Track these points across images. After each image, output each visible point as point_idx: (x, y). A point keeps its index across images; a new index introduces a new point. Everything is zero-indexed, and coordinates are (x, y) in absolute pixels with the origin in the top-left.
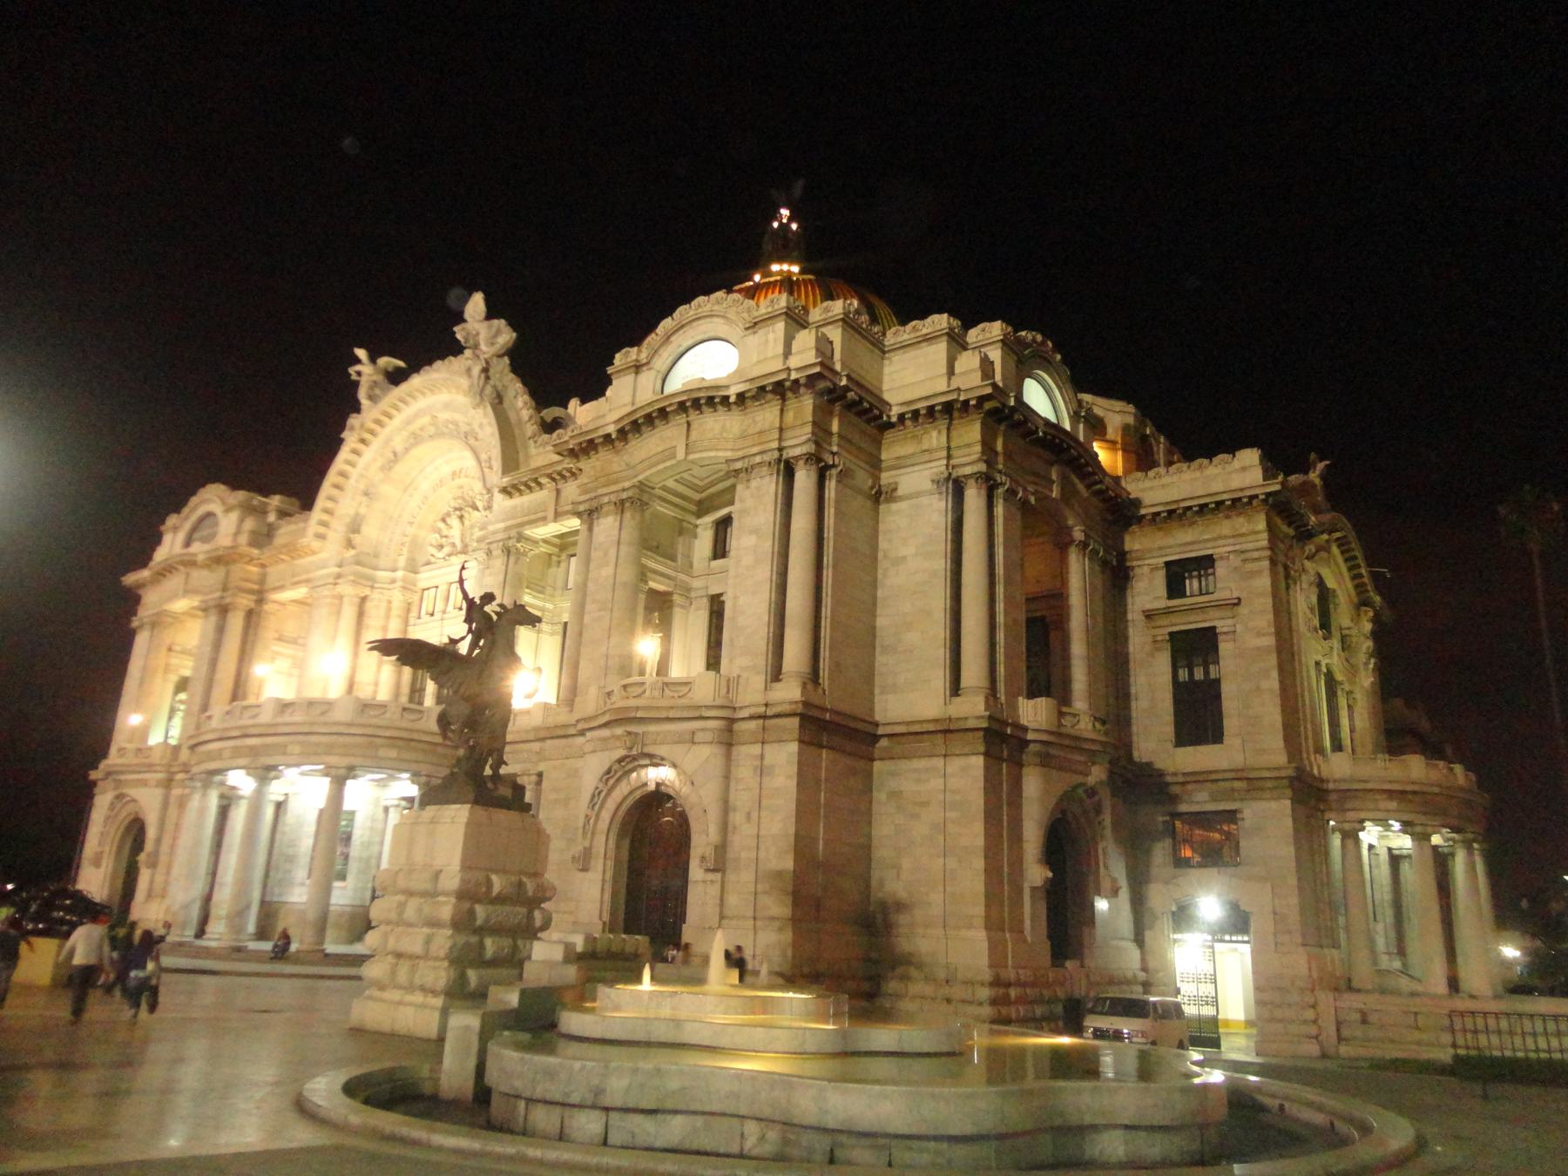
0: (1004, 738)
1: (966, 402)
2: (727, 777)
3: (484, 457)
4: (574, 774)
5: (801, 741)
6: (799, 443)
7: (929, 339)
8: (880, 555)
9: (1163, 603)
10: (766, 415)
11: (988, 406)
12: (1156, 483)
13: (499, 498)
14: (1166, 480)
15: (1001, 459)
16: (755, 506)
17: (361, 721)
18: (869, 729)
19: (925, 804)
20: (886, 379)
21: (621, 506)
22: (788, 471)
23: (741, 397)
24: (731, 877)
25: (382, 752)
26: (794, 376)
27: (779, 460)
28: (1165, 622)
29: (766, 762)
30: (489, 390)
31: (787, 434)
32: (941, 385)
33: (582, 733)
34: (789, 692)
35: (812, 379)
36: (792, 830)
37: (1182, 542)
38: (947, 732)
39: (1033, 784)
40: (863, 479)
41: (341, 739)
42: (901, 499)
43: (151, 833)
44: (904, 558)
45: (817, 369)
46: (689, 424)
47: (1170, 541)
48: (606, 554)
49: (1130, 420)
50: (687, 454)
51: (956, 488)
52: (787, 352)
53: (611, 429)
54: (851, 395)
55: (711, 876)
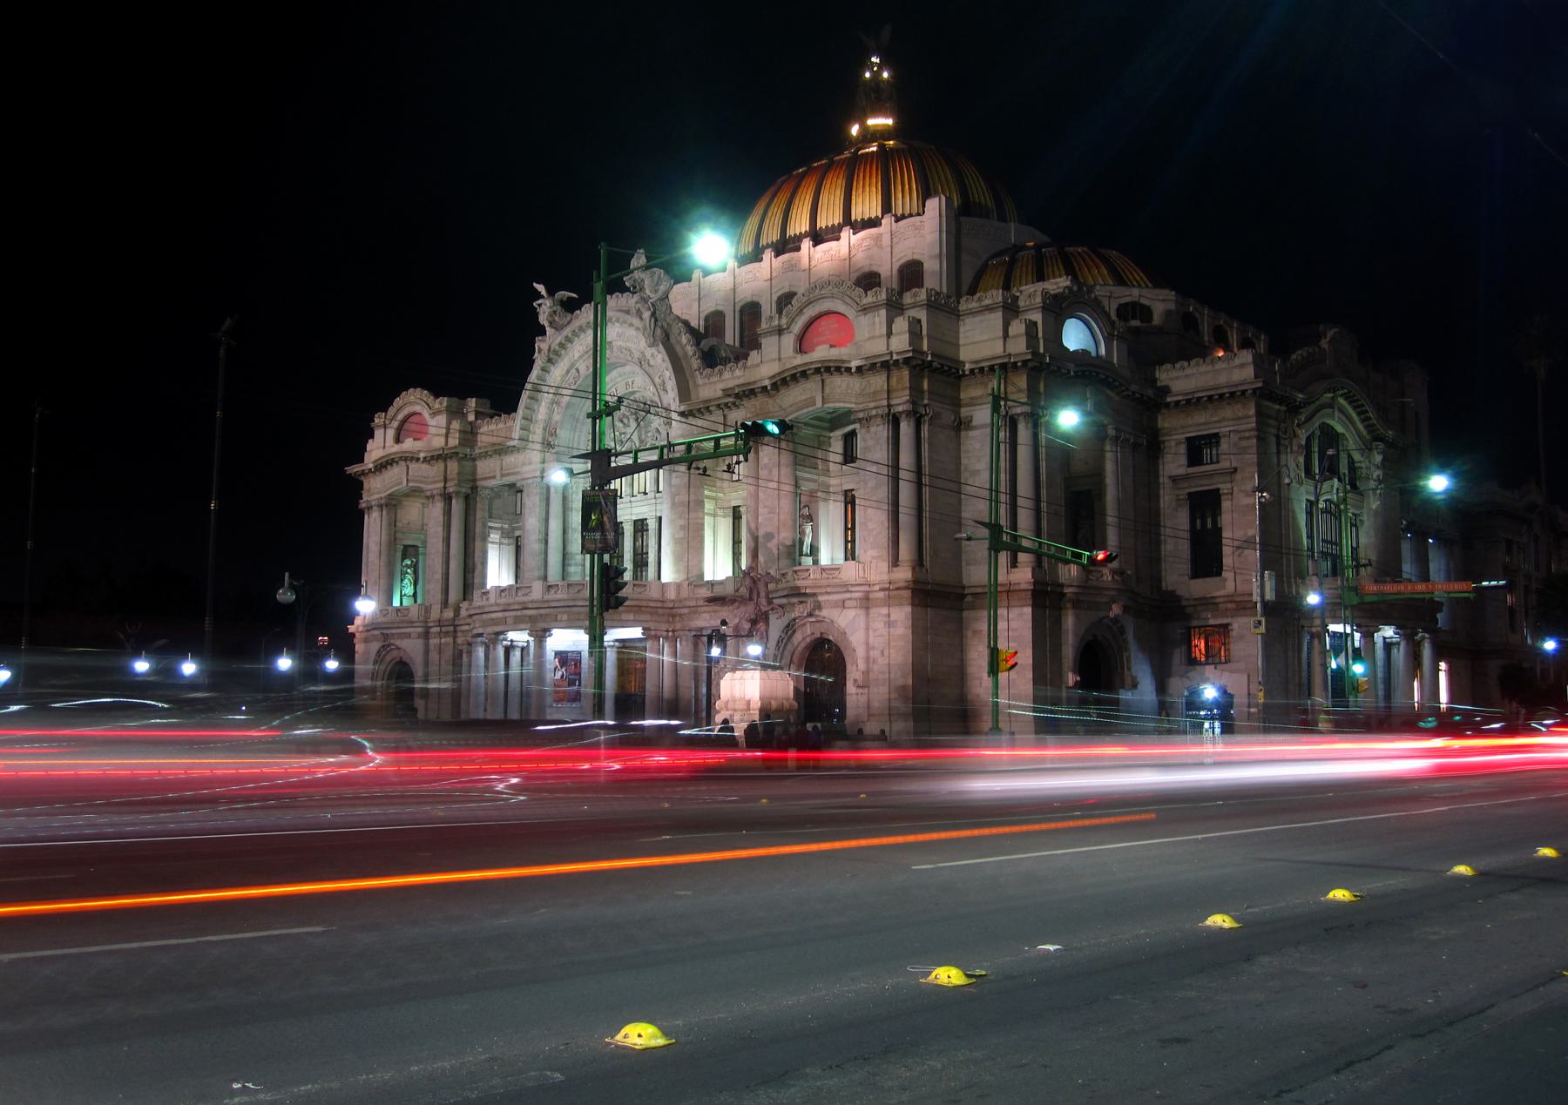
1: (1015, 364)
3: (657, 380)
6: (901, 402)
7: (989, 309)
9: (1182, 471)
10: (878, 381)
12: (1181, 373)
14: (1188, 371)
16: (874, 443)
23: (859, 369)
30: (659, 331)
31: (893, 395)
32: (998, 349)
34: (904, 574)
35: (907, 361)
37: (1198, 423)
39: (1069, 621)
40: (947, 417)
42: (975, 428)
49: (1172, 306)
52: (889, 334)
53: (767, 383)
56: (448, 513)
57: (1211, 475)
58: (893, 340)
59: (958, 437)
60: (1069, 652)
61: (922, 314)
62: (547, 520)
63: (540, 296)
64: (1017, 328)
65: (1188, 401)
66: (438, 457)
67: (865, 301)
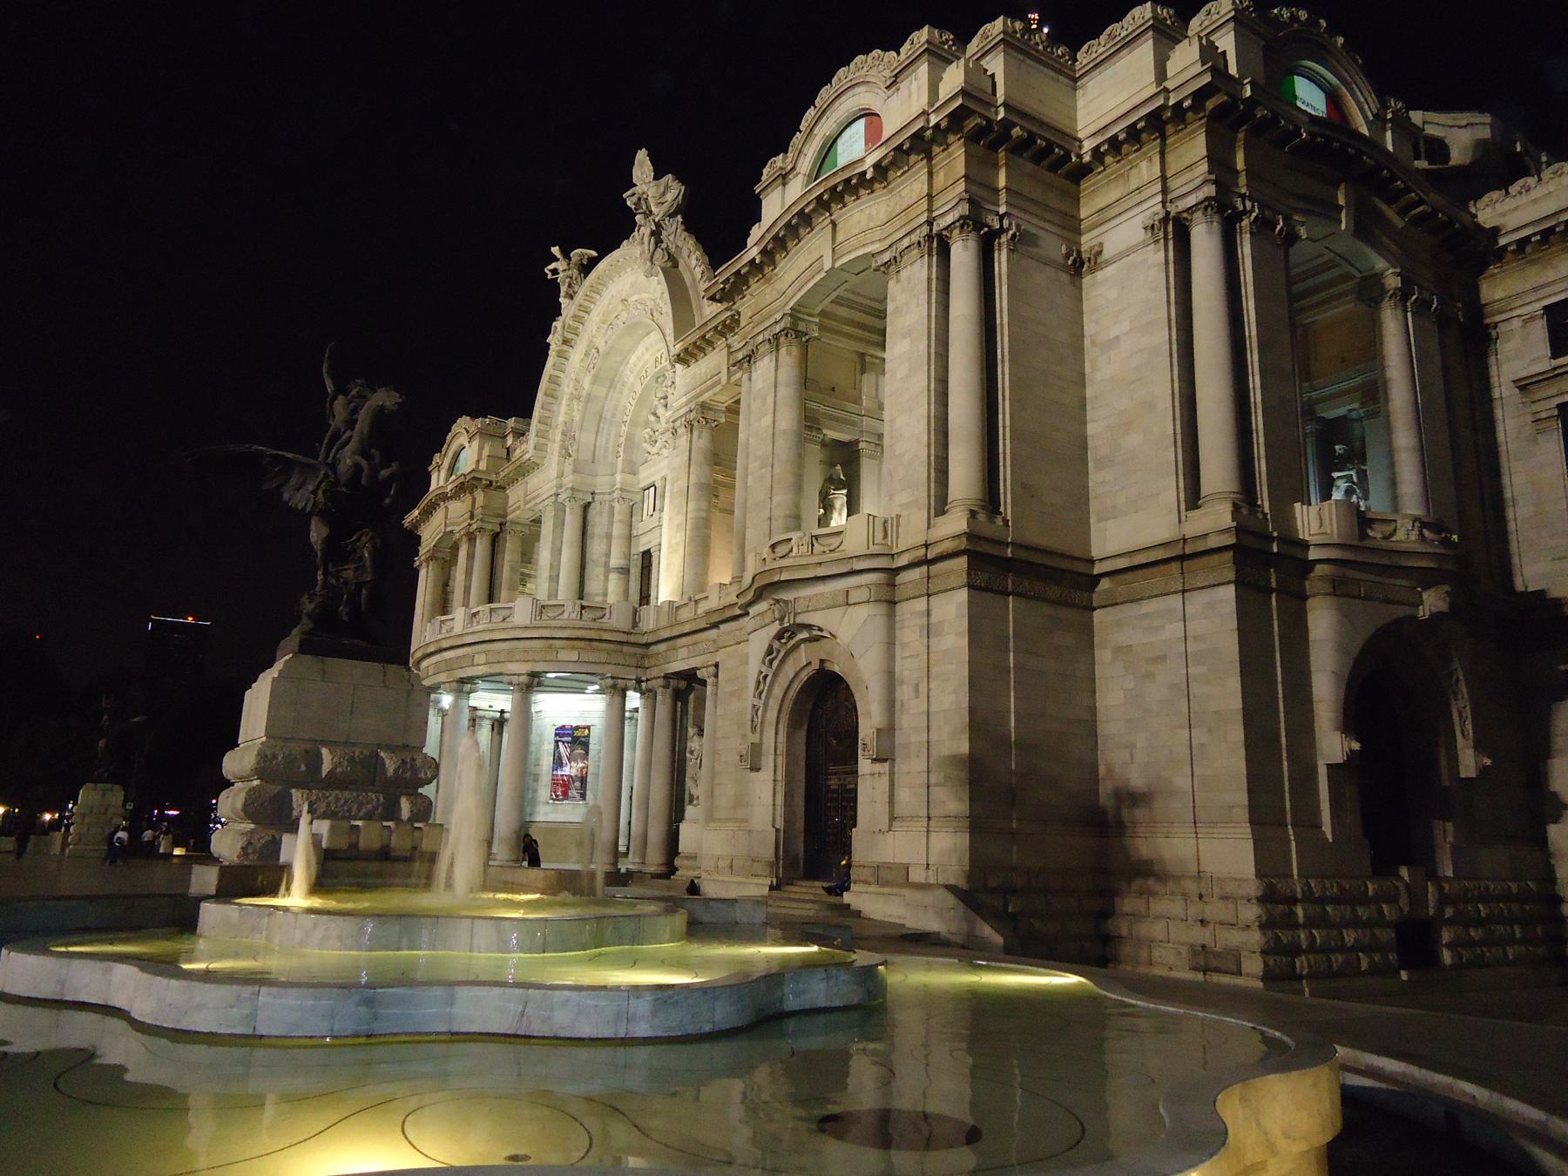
0: (1269, 560)
1: (1179, 104)
2: (891, 643)
5: (971, 586)
7: (1129, 43)
8: (1087, 342)
9: (1545, 365)
10: (912, 186)
11: (1210, 104)
12: (1524, 199)
15: (1243, 180)
17: (540, 623)
19: (1162, 658)
20: (1080, 114)
22: (940, 247)
24: (901, 766)
25: (563, 655)
26: (933, 120)
27: (930, 237)
28: (1553, 391)
29: (933, 620)
31: (936, 204)
34: (955, 523)
38: (1180, 558)
39: (1323, 623)
40: (1054, 247)
41: (522, 644)
42: (1109, 262)
44: (1117, 338)
46: (834, 224)
47: (1551, 275)
48: (764, 400)
50: (834, 261)
51: (1176, 231)
54: (1016, 132)
55: (878, 767)
56: (471, 557)
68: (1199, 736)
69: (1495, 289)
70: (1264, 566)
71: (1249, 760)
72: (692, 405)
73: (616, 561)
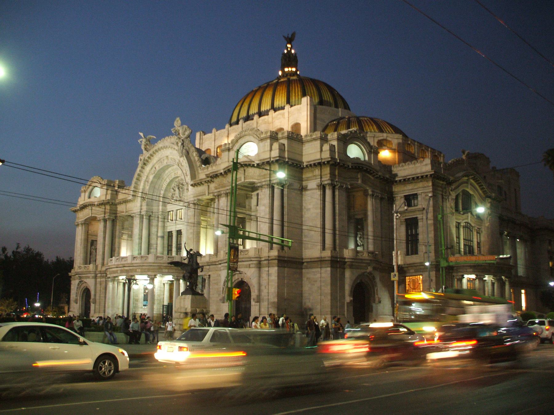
1: (324, 162)
2: (260, 276)
3: (184, 172)
4: (219, 275)
12: (402, 168)
13: (190, 188)
14: (405, 167)
17: (156, 261)
18: (300, 260)
21: (227, 194)
26: (272, 160)
29: (270, 272)
30: (184, 151)
32: (318, 157)
33: (220, 264)
36: (276, 291)
37: (409, 189)
38: (320, 261)
41: (152, 267)
43: (92, 293)
45: (278, 158)
46: (244, 170)
47: (405, 188)
49: (401, 141)
51: (323, 188)
52: (271, 150)
53: (222, 171)
55: (257, 304)
56: (105, 227)
57: (414, 211)
58: (273, 152)
59: (302, 194)
60: (347, 288)
61: (285, 142)
62: (142, 230)
63: (141, 138)
64: (326, 147)
65: (404, 180)
66: (102, 204)
67: (262, 136)
68: (323, 297)
69: (396, 189)
70: (337, 263)
71: (331, 303)
72: (196, 198)
73: (160, 234)
